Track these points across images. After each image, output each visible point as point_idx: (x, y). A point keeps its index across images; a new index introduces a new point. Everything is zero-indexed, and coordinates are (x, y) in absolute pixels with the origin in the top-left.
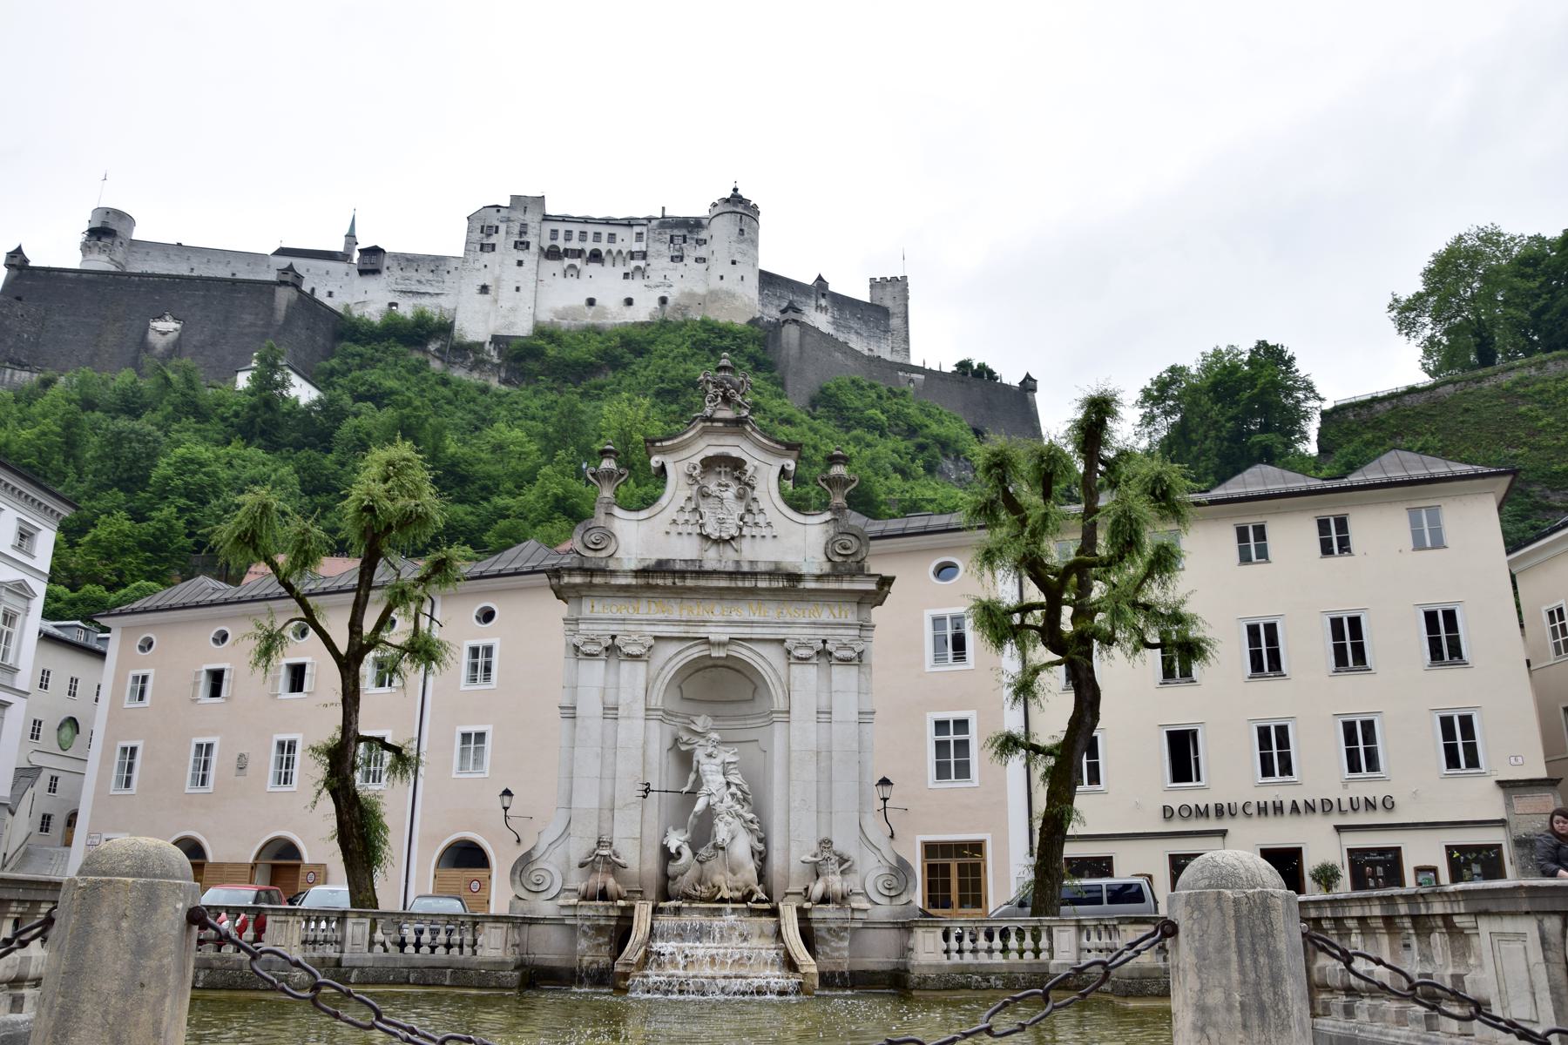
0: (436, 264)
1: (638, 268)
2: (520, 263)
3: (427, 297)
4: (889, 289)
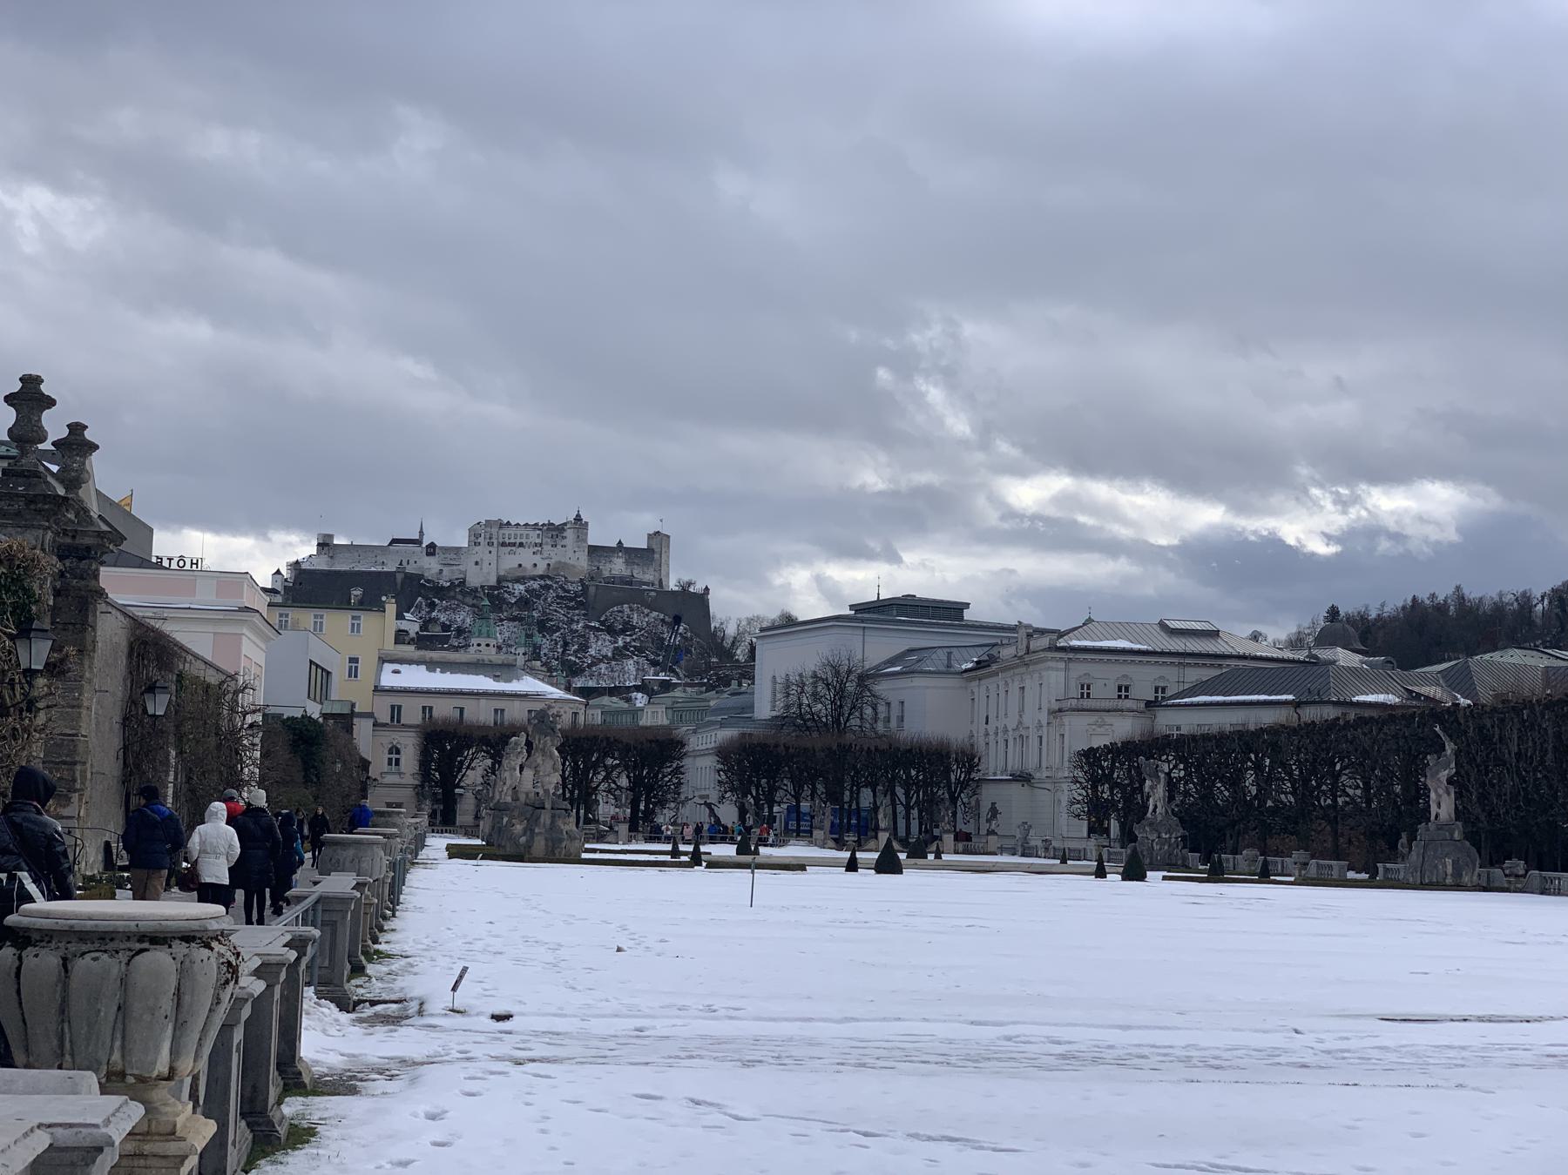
0: (457, 550)
1: (538, 551)
2: (490, 552)
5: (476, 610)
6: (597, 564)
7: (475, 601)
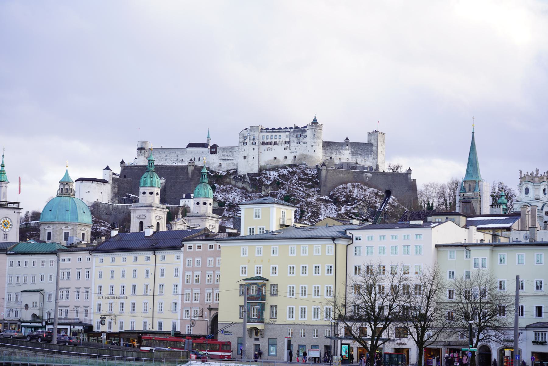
1: (287, 146)
2: (254, 149)
3: (230, 160)
4: (373, 136)
5: (244, 191)
6: (330, 155)
7: (244, 185)
